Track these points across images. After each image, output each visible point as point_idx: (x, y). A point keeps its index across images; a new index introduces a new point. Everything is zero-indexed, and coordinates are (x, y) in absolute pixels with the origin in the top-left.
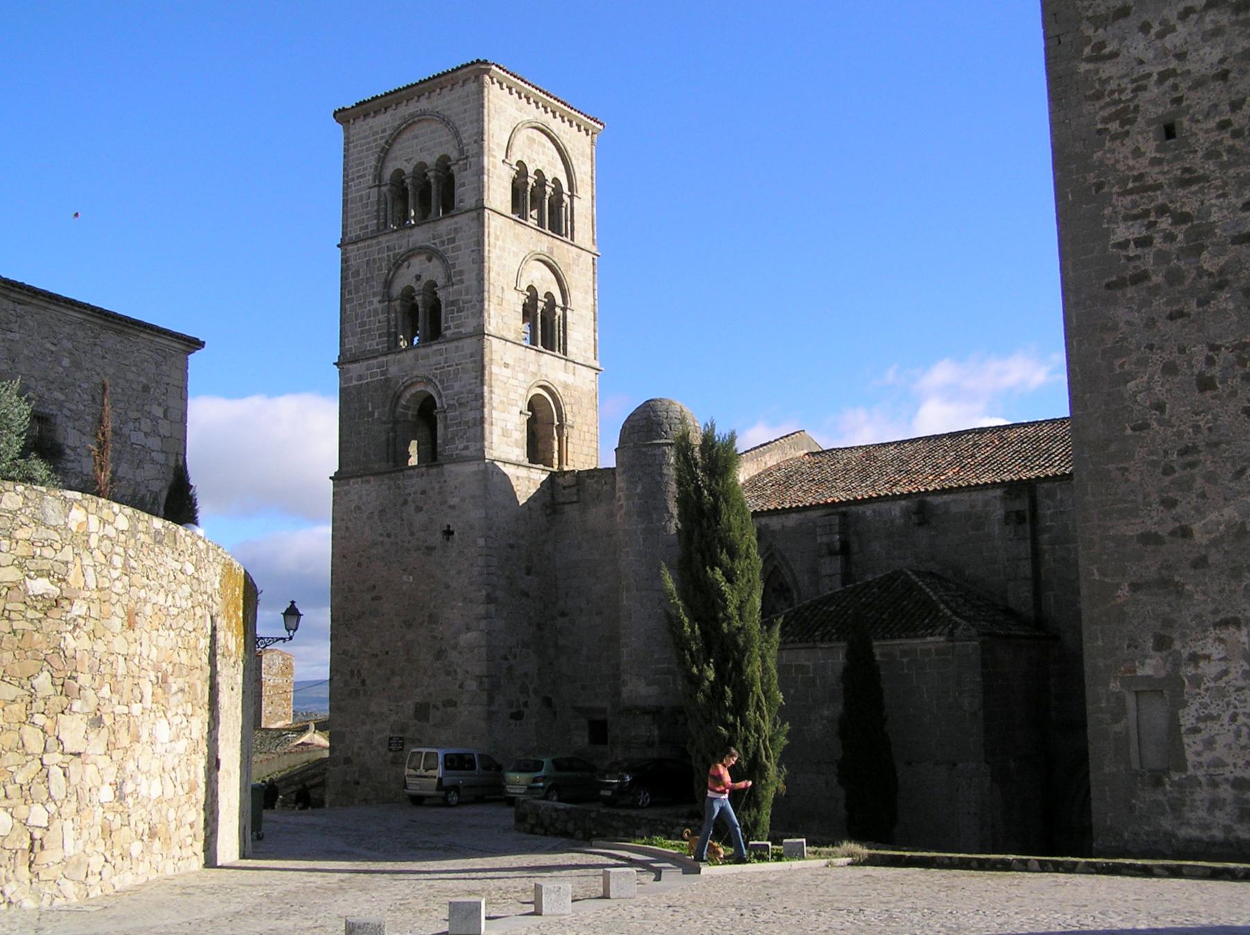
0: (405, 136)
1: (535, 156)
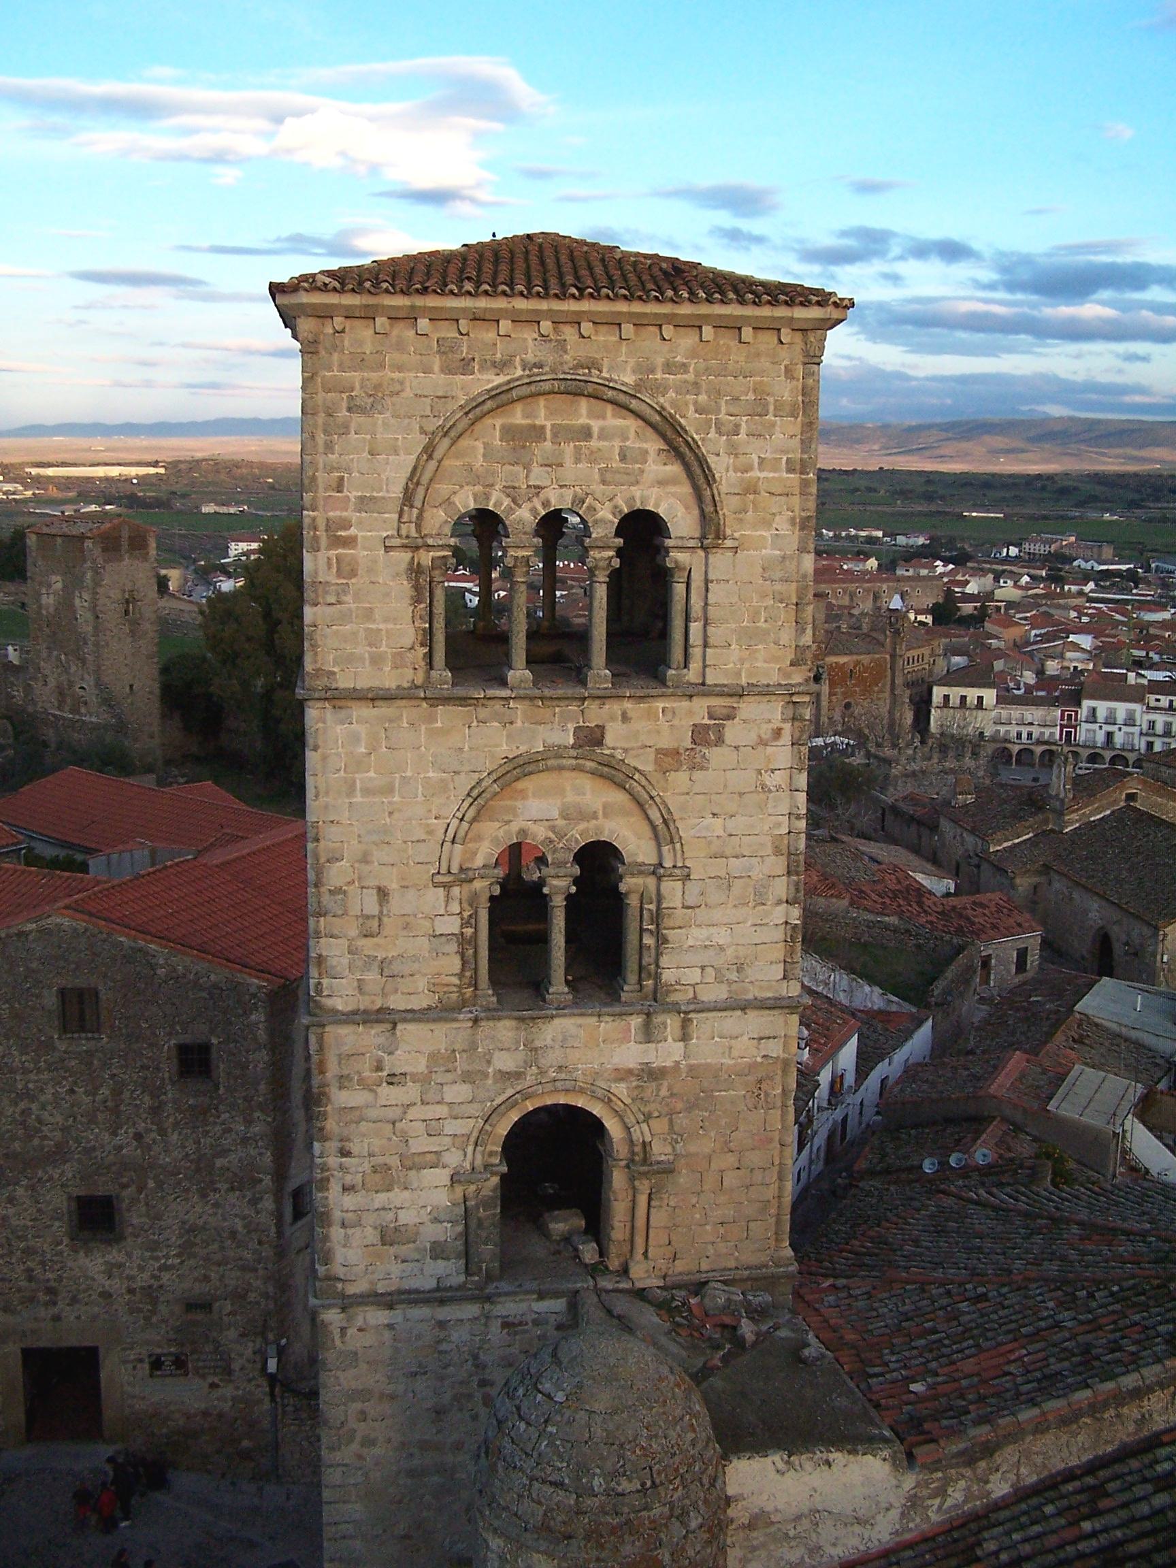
1: (538, 475)
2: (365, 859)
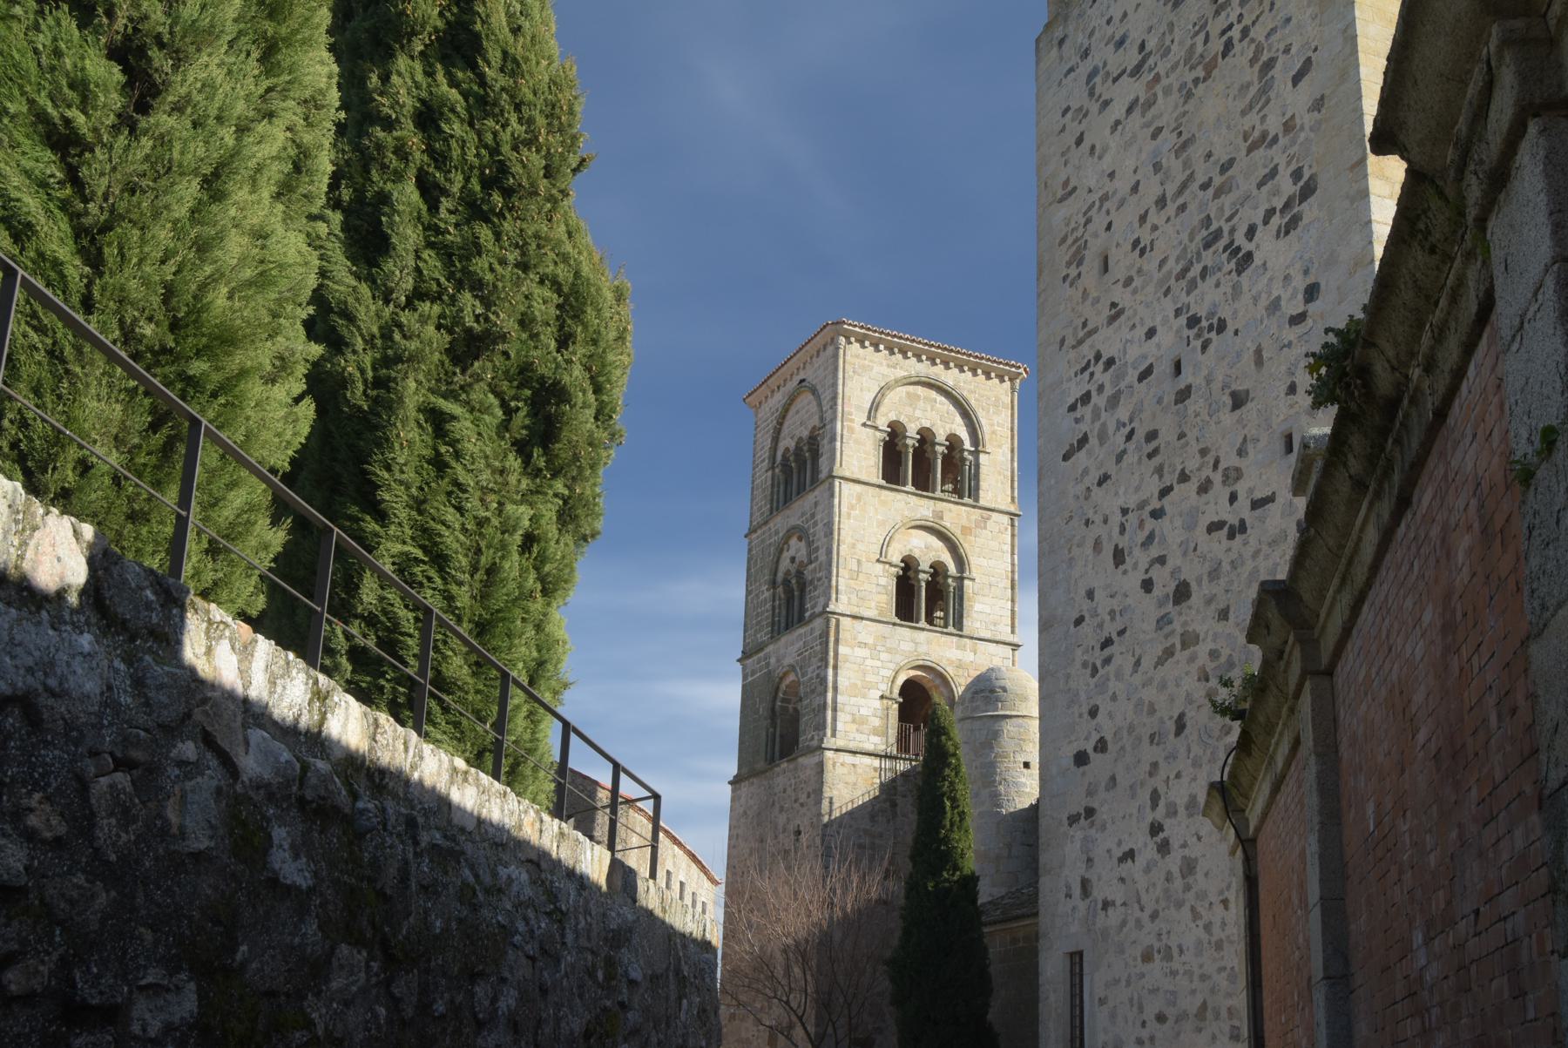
0: (790, 413)
1: (918, 413)
2: (853, 546)
